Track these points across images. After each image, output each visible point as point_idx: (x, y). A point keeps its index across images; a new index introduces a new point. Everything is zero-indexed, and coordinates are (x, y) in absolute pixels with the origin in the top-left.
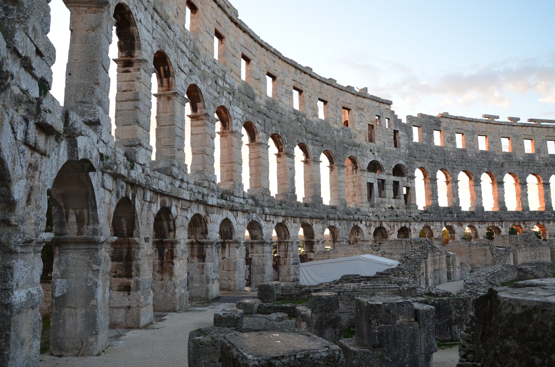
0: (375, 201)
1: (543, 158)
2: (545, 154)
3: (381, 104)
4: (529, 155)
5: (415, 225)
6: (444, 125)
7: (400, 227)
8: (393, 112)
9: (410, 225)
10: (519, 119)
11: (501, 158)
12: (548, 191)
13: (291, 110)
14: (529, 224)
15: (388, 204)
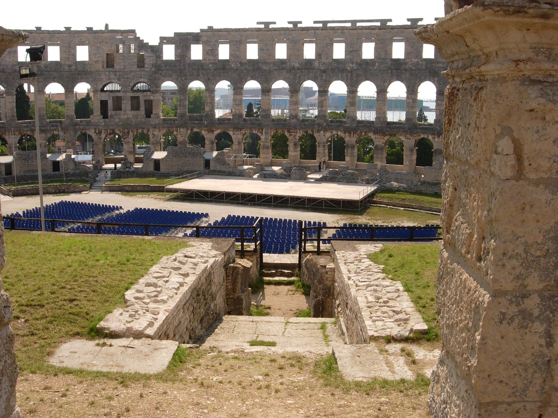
0: (109, 114)
1: (324, 63)
2: (327, 59)
3: (124, 34)
4: (310, 61)
5: (153, 131)
6: (204, 39)
7: (135, 133)
8: (139, 38)
9: (148, 130)
10: (301, 22)
11: (271, 66)
12: (323, 98)
13: (15, 63)
14: (294, 132)
15: (124, 115)
